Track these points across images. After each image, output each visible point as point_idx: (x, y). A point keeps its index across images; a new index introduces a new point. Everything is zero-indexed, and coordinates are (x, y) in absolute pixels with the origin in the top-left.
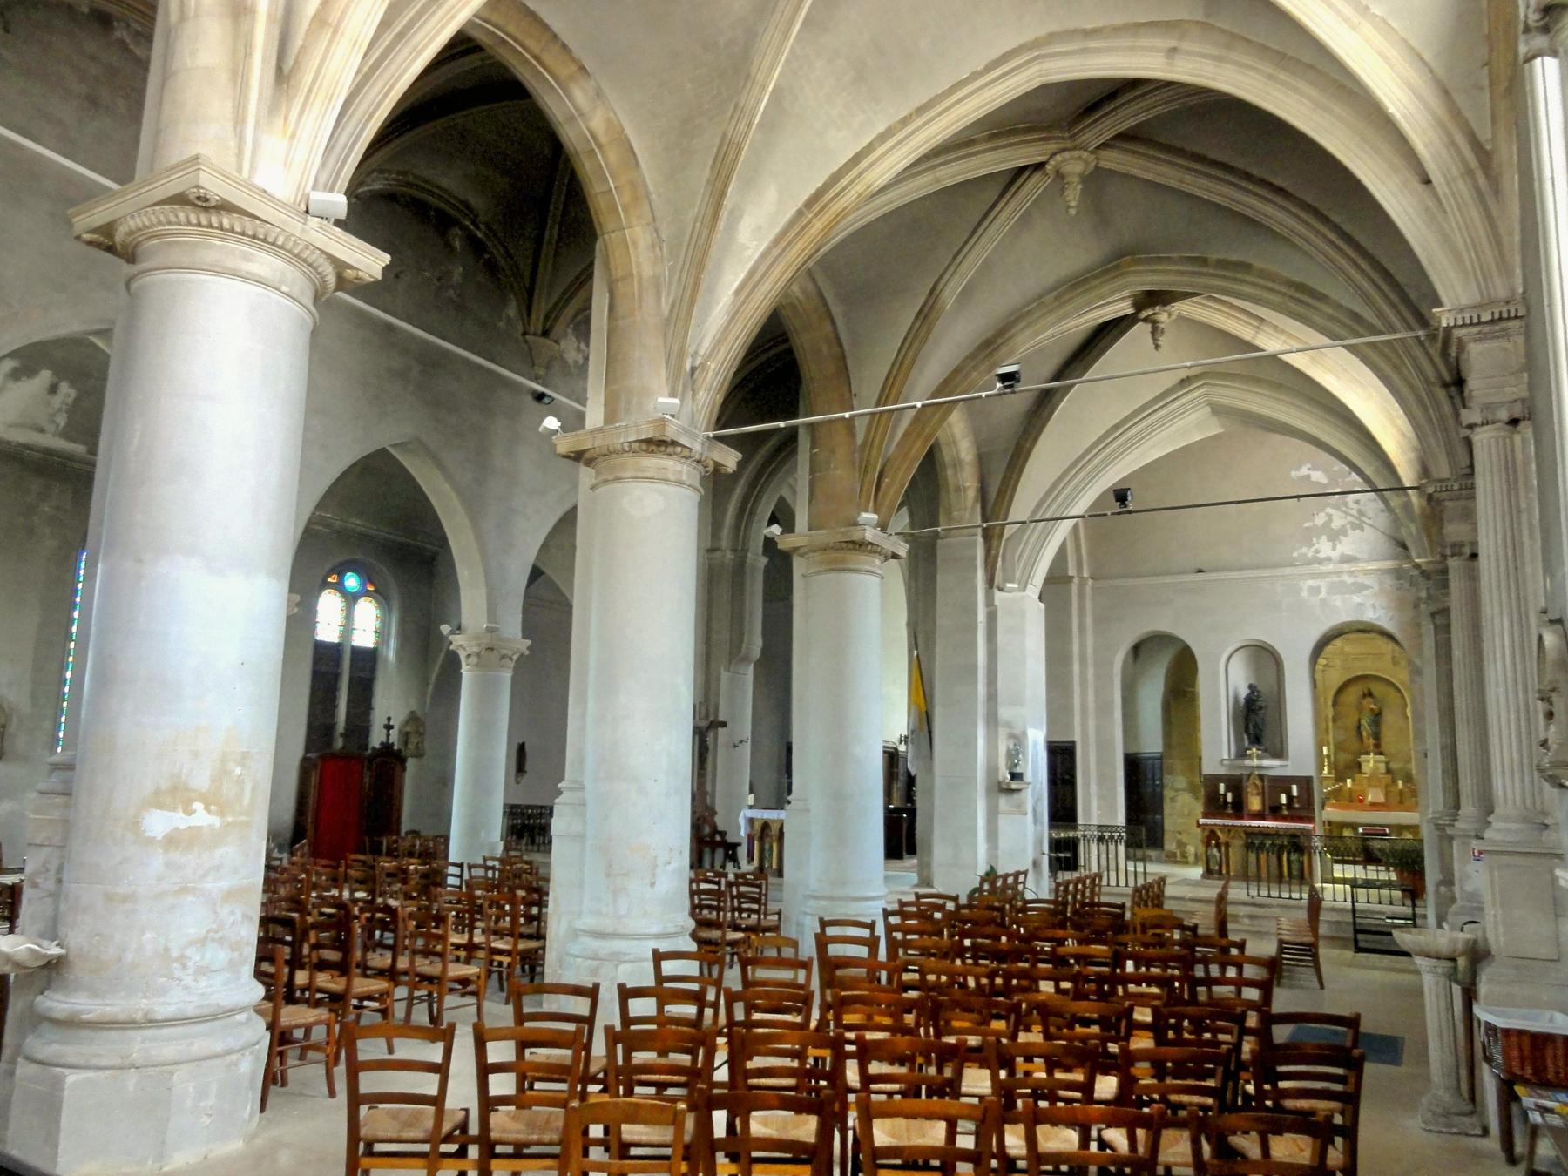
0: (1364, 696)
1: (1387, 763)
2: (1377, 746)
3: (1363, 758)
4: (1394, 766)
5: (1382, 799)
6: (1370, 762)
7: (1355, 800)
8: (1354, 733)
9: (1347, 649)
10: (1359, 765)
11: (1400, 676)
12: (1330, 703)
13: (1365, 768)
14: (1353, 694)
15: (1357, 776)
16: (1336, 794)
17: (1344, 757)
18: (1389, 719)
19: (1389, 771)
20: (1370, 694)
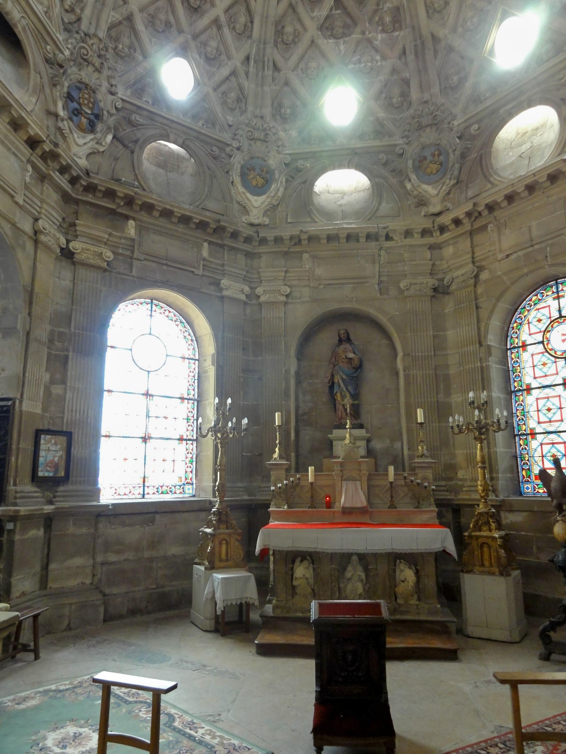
0: (340, 341)
1: (368, 441)
2: (356, 412)
3: (337, 433)
4: (377, 445)
5: (361, 501)
6: (346, 440)
7: (318, 506)
8: (325, 398)
9: (319, 271)
10: (330, 445)
11: (387, 311)
12: (293, 352)
13: (340, 449)
14: (326, 340)
15: (326, 461)
16: (289, 494)
17: (309, 435)
18: (373, 376)
19: (370, 453)
20: (348, 340)
